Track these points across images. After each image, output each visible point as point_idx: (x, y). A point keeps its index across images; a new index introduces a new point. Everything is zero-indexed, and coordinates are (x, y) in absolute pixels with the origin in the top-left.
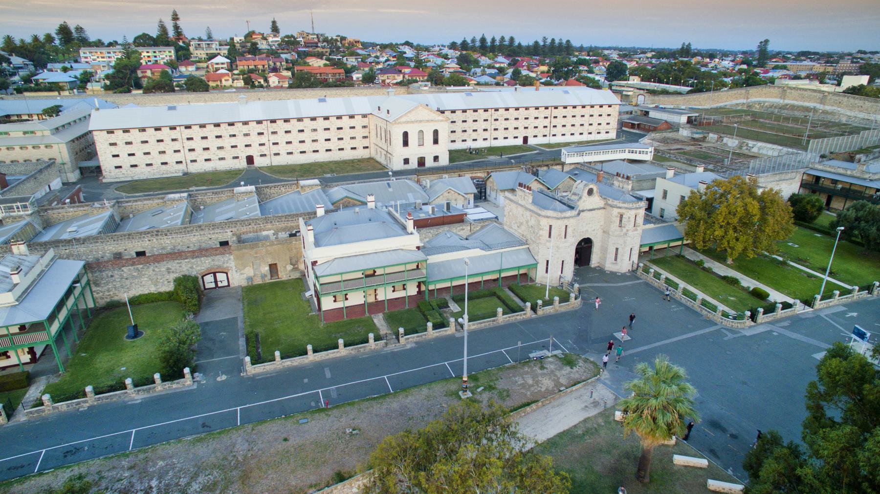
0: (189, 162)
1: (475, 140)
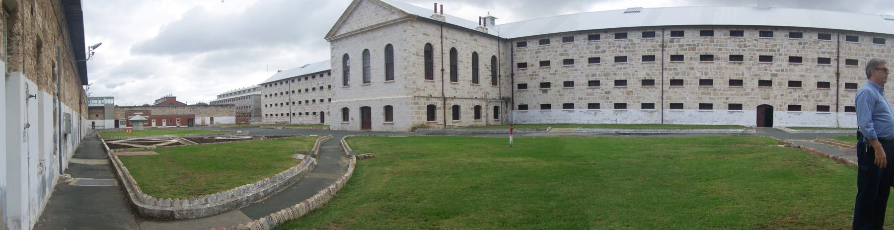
1: (621, 106)
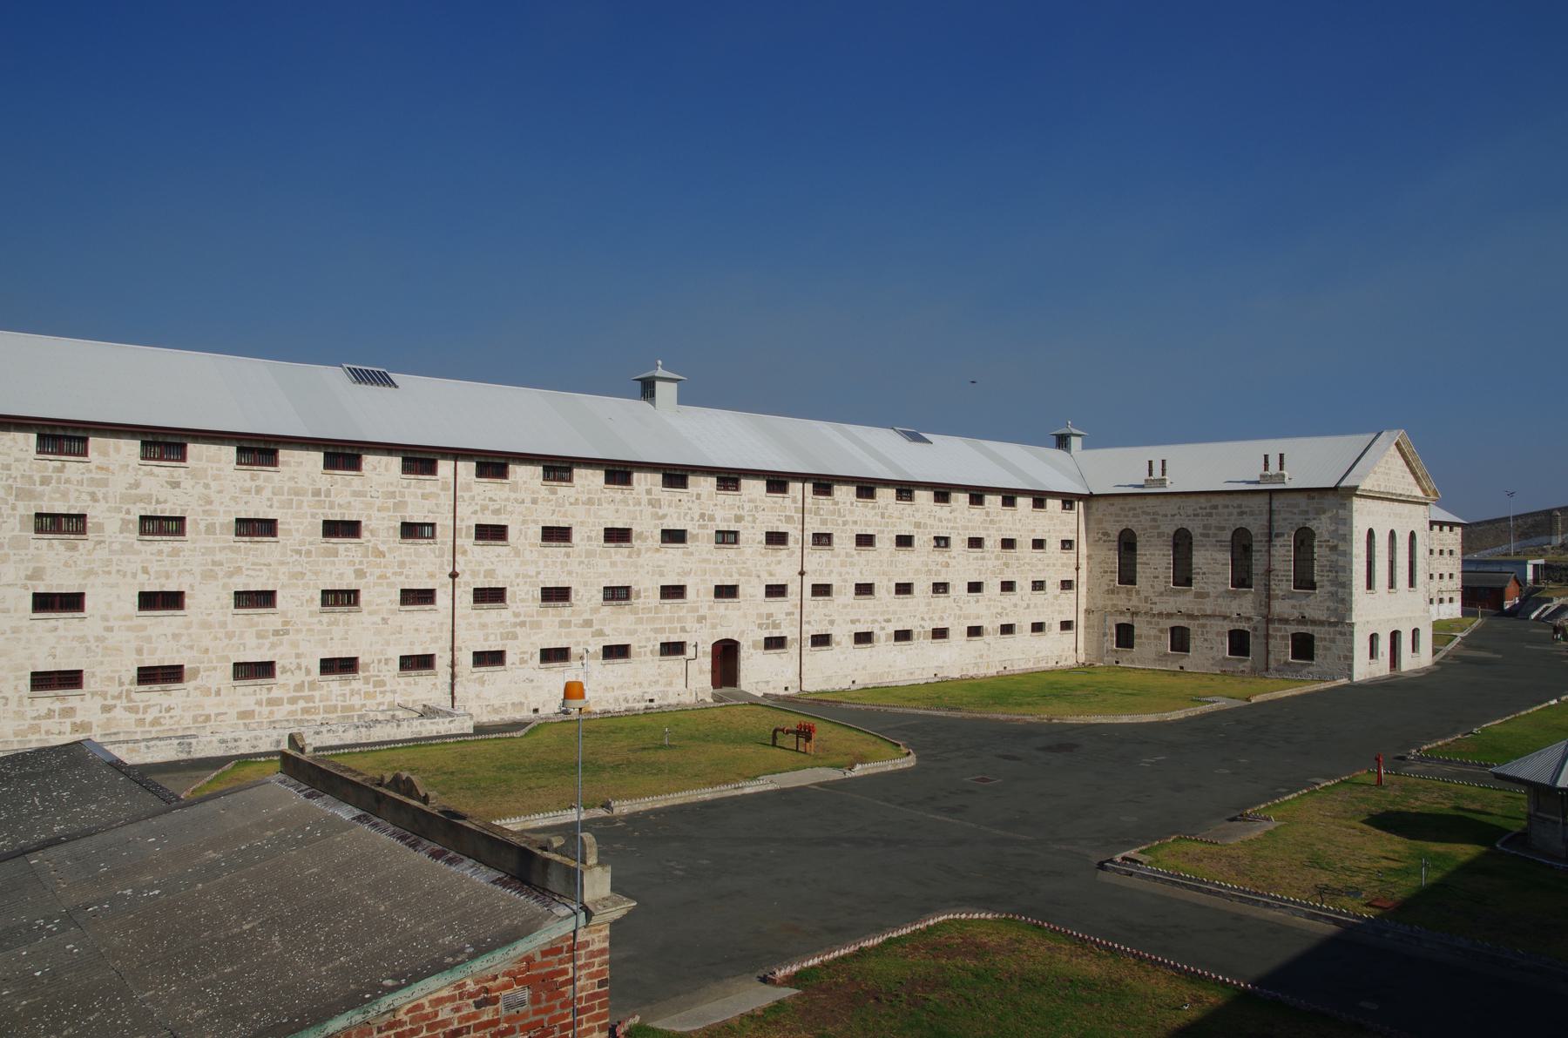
0: (465, 659)
